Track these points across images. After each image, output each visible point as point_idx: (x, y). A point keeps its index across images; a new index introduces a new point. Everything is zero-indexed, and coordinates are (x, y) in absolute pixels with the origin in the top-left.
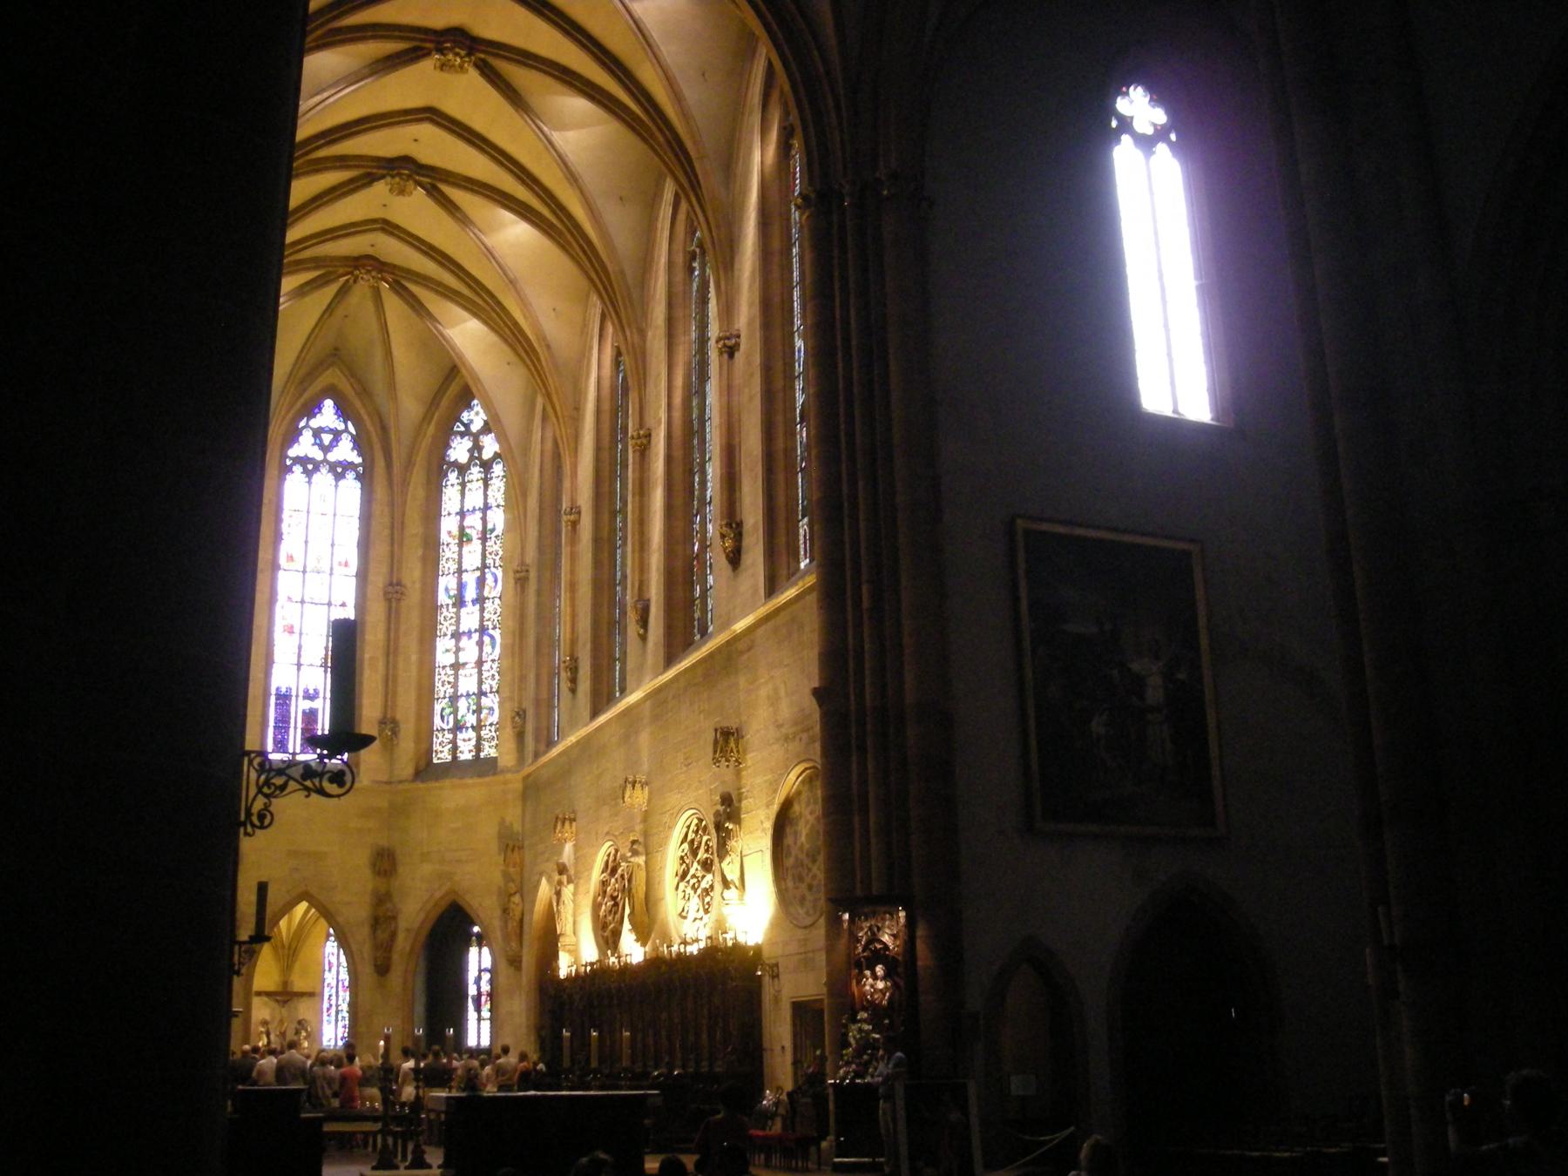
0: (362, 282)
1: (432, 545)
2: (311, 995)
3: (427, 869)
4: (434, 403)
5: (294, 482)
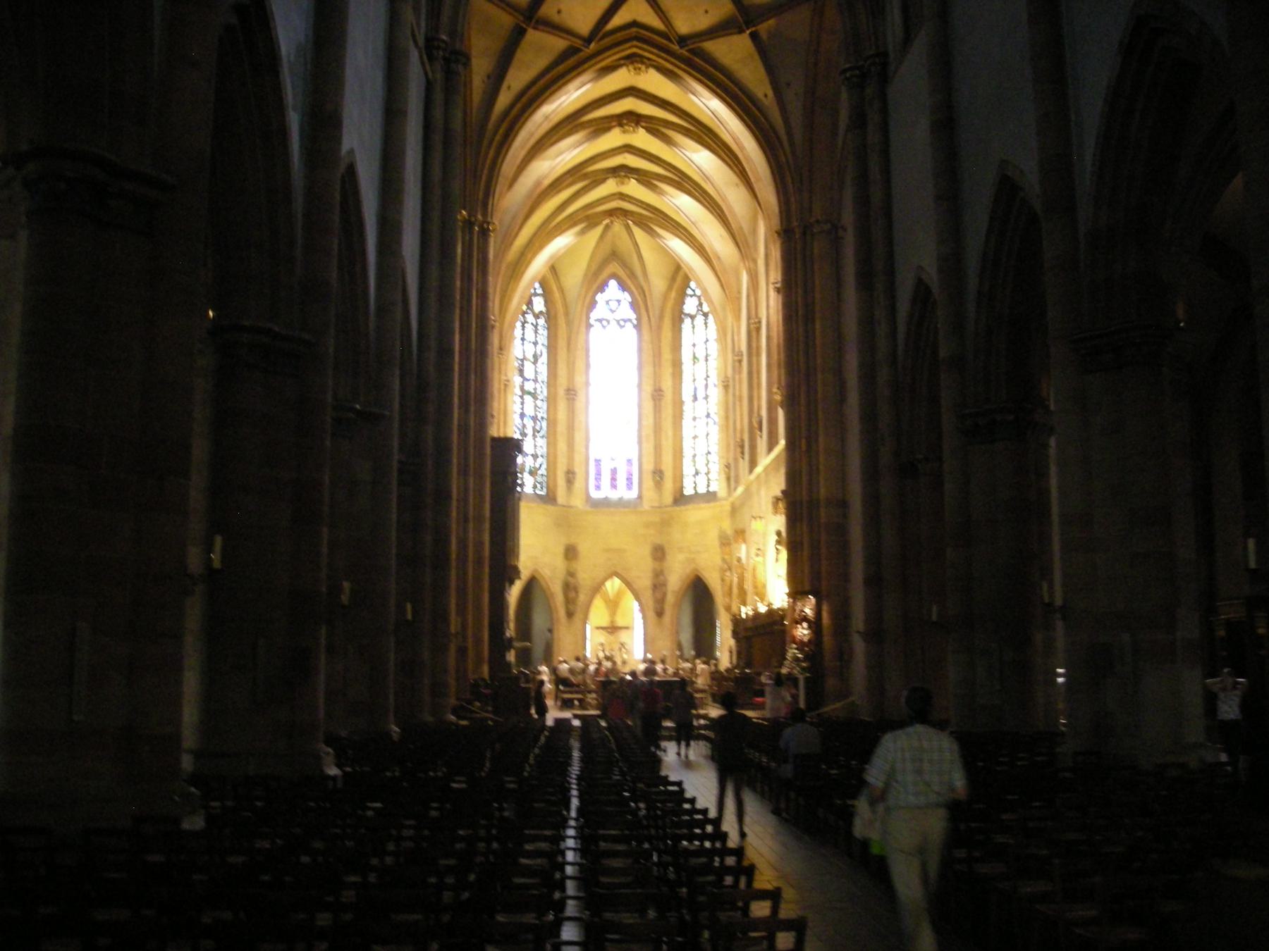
0: (616, 224)
1: (677, 365)
2: (627, 628)
3: (681, 557)
4: (673, 279)
5: (596, 334)
